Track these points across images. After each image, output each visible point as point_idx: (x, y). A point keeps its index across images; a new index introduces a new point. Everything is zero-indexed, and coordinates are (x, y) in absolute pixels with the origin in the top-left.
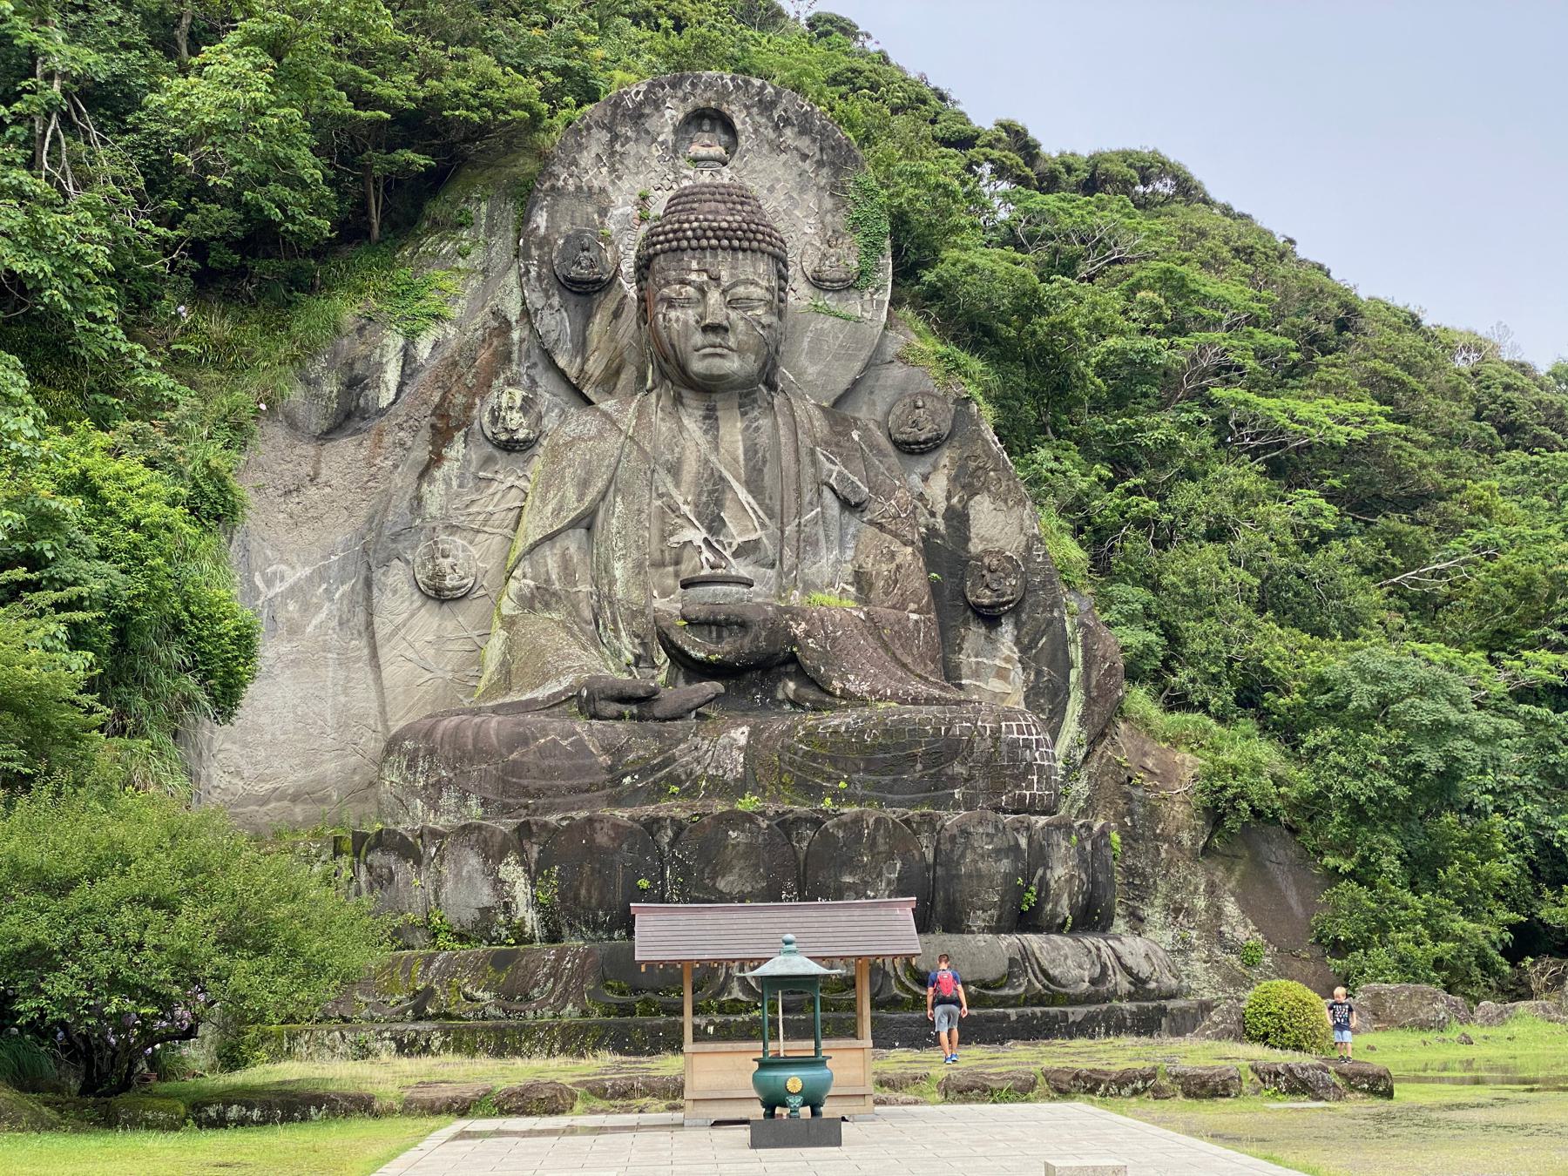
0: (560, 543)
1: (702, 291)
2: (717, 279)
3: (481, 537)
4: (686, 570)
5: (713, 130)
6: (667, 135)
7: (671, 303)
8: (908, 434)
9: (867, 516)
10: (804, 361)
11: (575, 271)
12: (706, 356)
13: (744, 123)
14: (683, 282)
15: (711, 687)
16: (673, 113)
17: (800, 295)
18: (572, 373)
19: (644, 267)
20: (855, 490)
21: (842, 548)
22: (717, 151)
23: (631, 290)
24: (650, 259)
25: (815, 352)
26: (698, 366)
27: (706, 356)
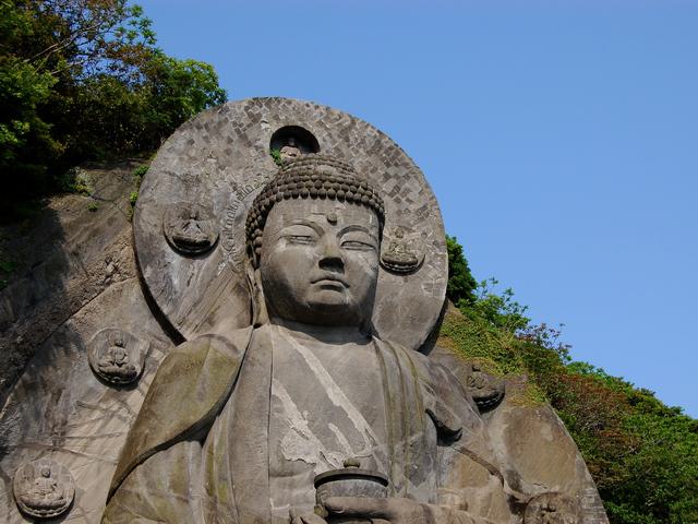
0: (175, 450)
1: (321, 232)
3: (80, 461)
12: (324, 287)
13: (324, 140)
26: (313, 296)
27: (324, 287)
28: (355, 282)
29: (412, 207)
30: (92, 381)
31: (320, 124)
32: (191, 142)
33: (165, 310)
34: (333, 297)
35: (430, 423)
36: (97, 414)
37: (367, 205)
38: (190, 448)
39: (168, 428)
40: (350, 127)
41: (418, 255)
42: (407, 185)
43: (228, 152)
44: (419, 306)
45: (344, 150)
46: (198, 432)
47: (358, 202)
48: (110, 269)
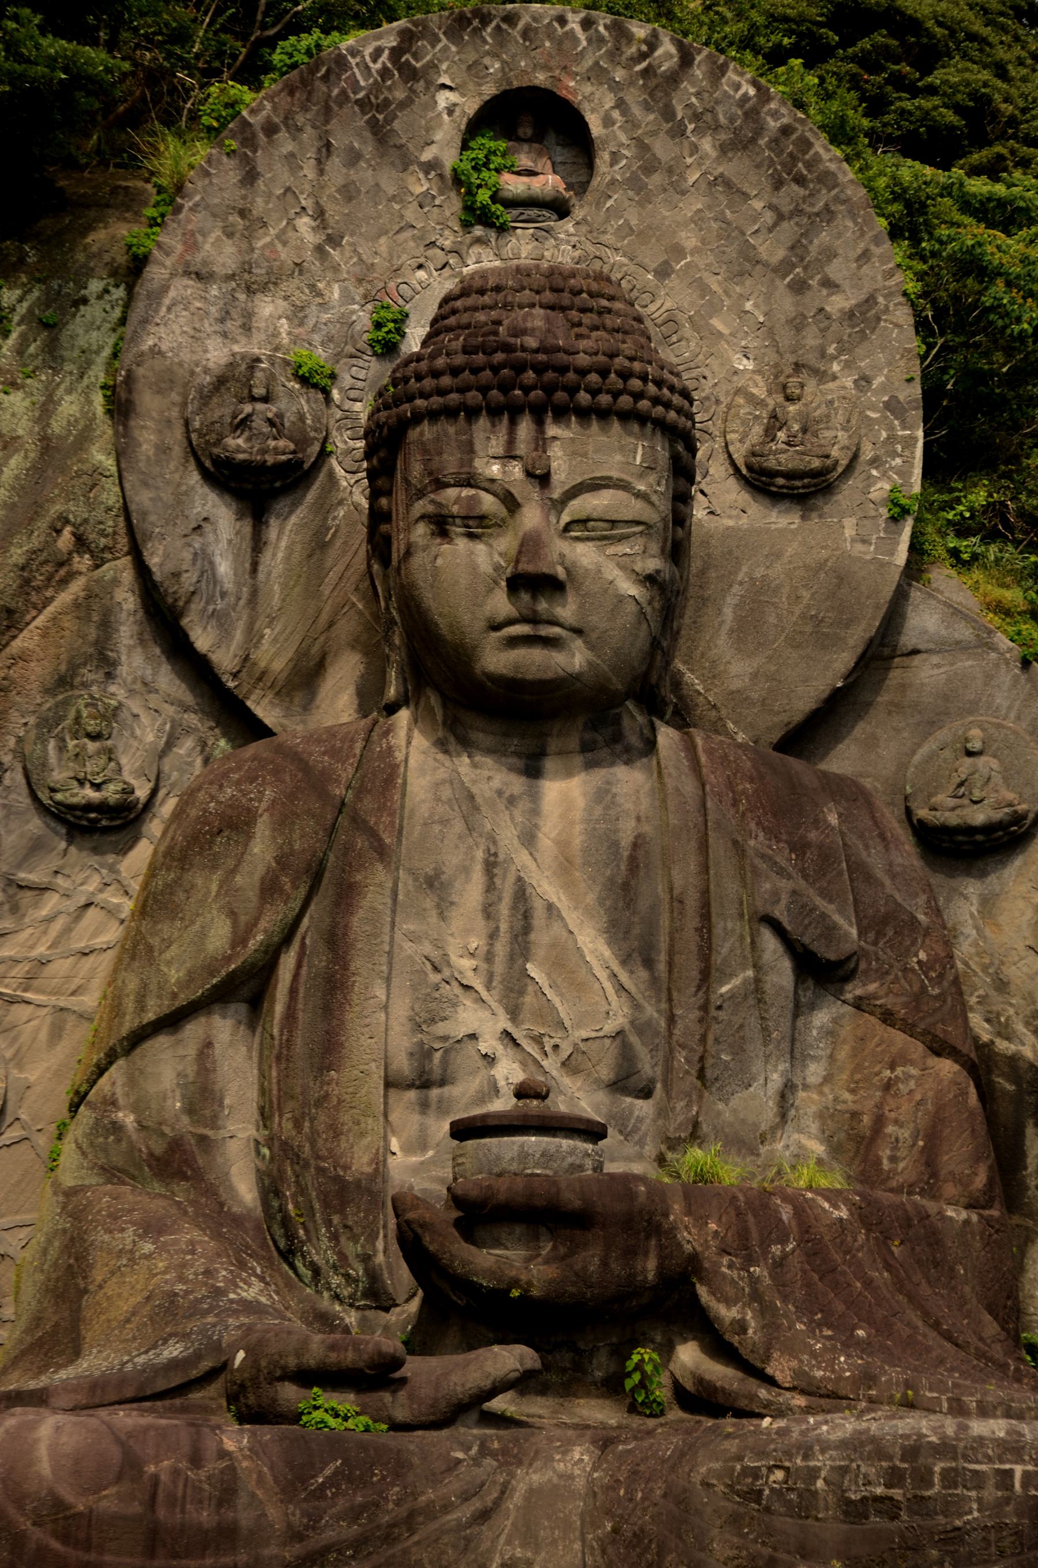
0: (193, 1030)
1: (511, 503)
2: (544, 480)
4: (464, 1098)
5: (537, 138)
6: (443, 146)
7: (441, 525)
8: (945, 810)
9: (854, 990)
10: (722, 645)
11: (237, 444)
14: (470, 481)
15: (509, 1358)
16: (453, 103)
17: (722, 504)
18: (224, 660)
19: (385, 446)
20: (830, 931)
21: (795, 1052)
22: (549, 183)
23: (350, 486)
24: (404, 425)
25: (748, 628)
26: (496, 660)
28: (597, 620)
29: (838, 304)
30: (36, 824)
31: (597, 74)
32: (250, 177)
33: (202, 640)
34: (535, 662)
35: (770, 942)
36: (51, 903)
37: (626, 417)
38: (223, 1028)
39: (176, 971)
40: (673, 79)
41: (836, 441)
42: (824, 237)
43: (348, 193)
44: (839, 578)
45: (662, 148)
46: (245, 988)
47: (604, 415)
48: (66, 540)
